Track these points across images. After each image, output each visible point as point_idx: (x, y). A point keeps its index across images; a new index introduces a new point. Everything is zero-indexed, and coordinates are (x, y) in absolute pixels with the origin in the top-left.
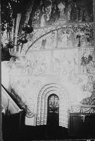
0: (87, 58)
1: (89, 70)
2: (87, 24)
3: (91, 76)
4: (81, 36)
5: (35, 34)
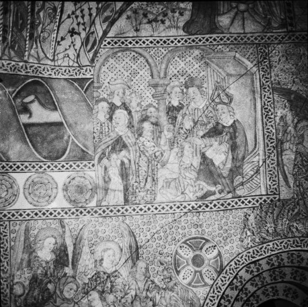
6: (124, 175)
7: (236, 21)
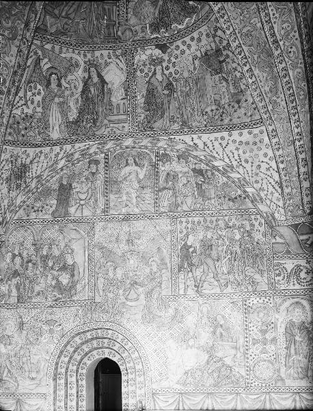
2: (194, 136)
4: (180, 175)
5: (31, 162)
6: (18, 289)
7: (78, 210)
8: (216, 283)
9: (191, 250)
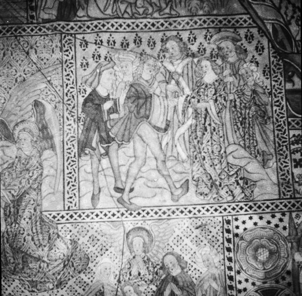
0: (122, 101)
1: (132, 190)
3: (139, 228)
8: (161, 182)
9: (107, 106)
